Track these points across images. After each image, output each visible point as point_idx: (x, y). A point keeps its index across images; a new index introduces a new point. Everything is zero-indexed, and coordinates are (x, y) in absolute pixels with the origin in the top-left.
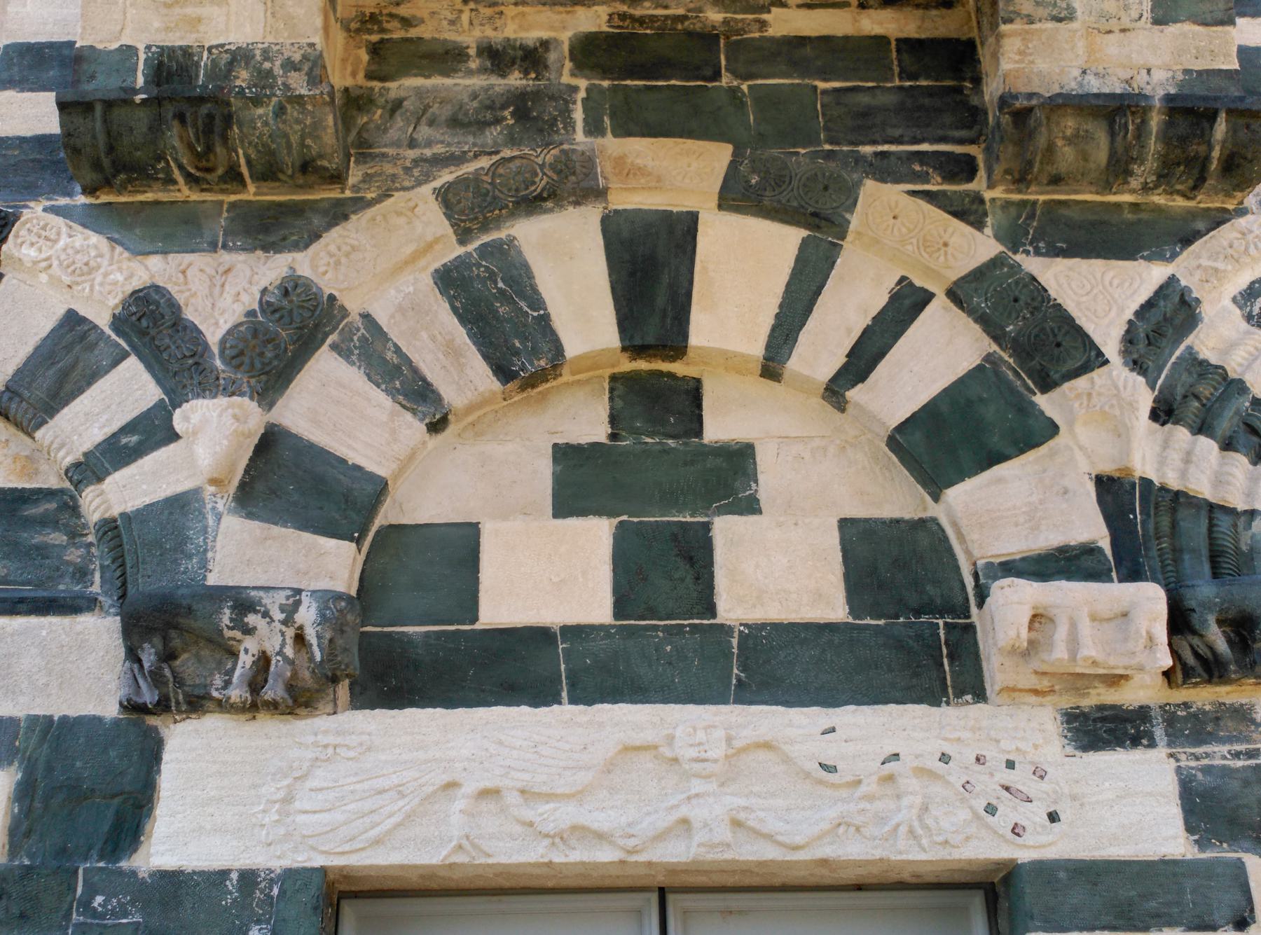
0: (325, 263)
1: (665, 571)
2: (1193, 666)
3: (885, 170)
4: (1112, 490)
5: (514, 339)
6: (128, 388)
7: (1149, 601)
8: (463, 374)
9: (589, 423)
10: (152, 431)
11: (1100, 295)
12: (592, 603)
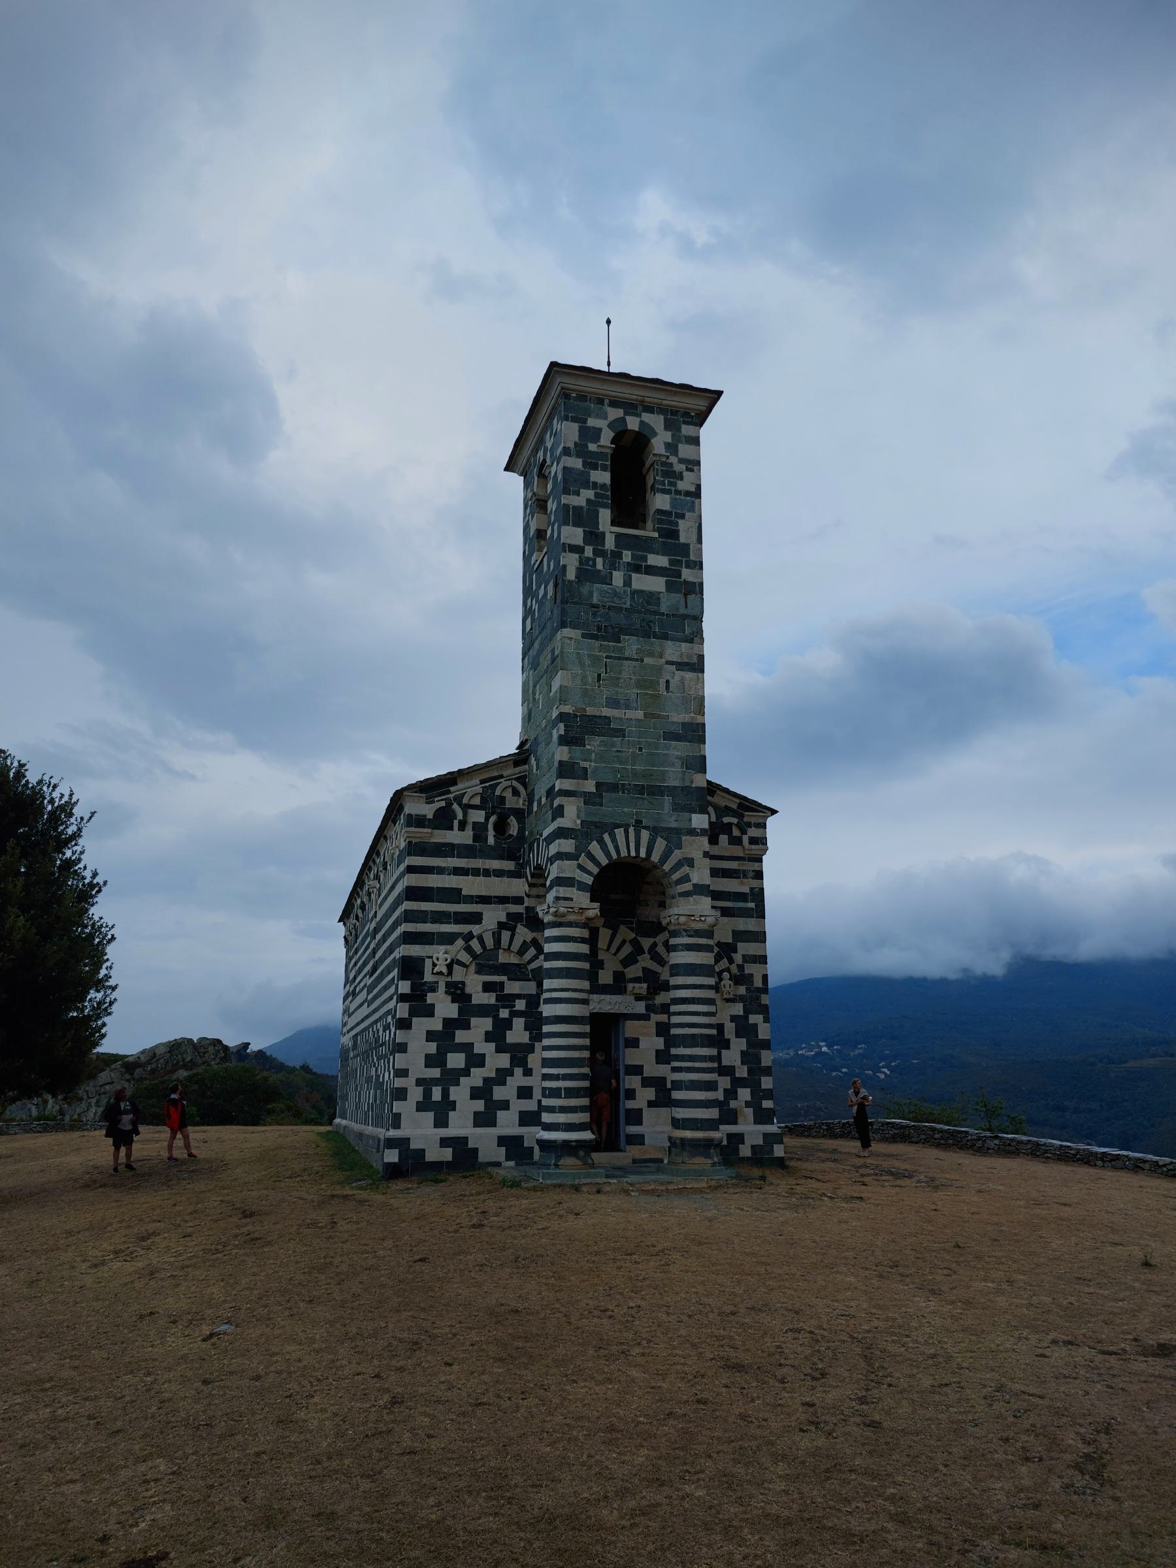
2: (649, 992)
3: (624, 923)
4: (644, 969)
7: (645, 985)
11: (646, 943)
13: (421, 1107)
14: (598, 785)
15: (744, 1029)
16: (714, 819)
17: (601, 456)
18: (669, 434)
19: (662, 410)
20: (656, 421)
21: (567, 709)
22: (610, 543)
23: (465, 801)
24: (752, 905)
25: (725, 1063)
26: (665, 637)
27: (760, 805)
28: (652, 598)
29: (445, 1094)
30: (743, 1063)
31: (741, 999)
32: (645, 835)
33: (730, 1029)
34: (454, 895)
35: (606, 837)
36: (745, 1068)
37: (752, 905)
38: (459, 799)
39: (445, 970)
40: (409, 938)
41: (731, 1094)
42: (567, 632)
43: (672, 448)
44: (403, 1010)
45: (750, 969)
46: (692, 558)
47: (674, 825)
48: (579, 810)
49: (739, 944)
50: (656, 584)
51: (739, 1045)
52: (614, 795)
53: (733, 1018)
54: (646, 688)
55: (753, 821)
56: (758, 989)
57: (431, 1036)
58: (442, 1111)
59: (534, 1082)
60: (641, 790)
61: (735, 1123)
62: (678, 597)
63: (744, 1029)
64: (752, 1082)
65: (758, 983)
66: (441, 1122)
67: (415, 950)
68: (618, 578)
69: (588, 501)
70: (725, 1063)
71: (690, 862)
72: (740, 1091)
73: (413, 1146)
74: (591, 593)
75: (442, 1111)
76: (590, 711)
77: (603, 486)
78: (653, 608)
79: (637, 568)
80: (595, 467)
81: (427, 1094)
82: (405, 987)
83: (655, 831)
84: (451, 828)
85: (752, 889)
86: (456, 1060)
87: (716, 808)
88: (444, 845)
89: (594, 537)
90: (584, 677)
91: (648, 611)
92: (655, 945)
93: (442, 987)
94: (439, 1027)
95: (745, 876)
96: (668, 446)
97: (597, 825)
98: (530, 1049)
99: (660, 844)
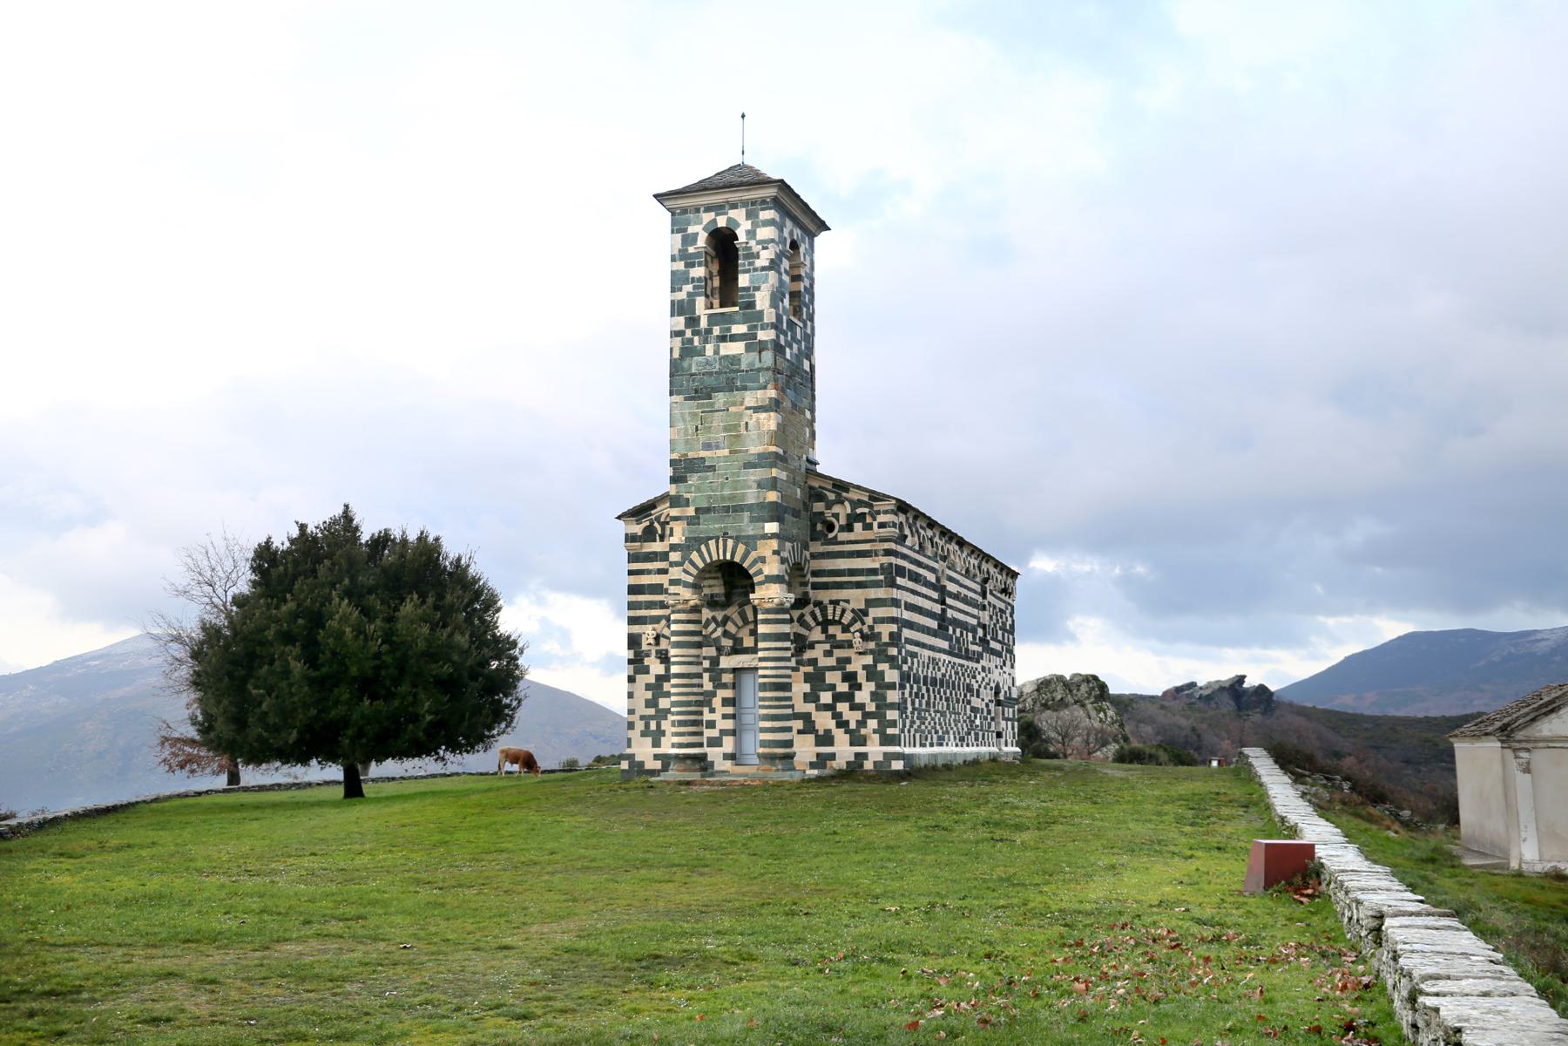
8: (740, 623)
13: (644, 734)
14: (697, 510)
15: (872, 673)
17: (697, 255)
19: (744, 204)
20: (739, 215)
21: (675, 456)
24: (881, 577)
25: (857, 700)
26: (745, 388)
28: (735, 359)
29: (659, 725)
31: (872, 652)
32: (730, 543)
34: (658, 589)
37: (881, 577)
38: (658, 519)
41: (862, 723)
42: (676, 398)
43: (751, 234)
50: (736, 348)
51: (869, 687)
53: (865, 667)
56: (887, 645)
57: (648, 687)
58: (657, 737)
59: (716, 717)
61: (864, 744)
62: (755, 355)
64: (879, 715)
65: (885, 639)
66: (656, 744)
67: (636, 629)
69: (689, 294)
70: (857, 700)
71: (763, 560)
73: (637, 759)
76: (691, 455)
77: (699, 279)
79: (723, 339)
80: (692, 265)
81: (647, 725)
83: (737, 539)
86: (664, 703)
87: (851, 502)
89: (692, 321)
90: (686, 430)
91: (732, 371)
92: (802, 615)
96: (748, 232)
97: (695, 539)
98: (714, 694)
99: (741, 548)
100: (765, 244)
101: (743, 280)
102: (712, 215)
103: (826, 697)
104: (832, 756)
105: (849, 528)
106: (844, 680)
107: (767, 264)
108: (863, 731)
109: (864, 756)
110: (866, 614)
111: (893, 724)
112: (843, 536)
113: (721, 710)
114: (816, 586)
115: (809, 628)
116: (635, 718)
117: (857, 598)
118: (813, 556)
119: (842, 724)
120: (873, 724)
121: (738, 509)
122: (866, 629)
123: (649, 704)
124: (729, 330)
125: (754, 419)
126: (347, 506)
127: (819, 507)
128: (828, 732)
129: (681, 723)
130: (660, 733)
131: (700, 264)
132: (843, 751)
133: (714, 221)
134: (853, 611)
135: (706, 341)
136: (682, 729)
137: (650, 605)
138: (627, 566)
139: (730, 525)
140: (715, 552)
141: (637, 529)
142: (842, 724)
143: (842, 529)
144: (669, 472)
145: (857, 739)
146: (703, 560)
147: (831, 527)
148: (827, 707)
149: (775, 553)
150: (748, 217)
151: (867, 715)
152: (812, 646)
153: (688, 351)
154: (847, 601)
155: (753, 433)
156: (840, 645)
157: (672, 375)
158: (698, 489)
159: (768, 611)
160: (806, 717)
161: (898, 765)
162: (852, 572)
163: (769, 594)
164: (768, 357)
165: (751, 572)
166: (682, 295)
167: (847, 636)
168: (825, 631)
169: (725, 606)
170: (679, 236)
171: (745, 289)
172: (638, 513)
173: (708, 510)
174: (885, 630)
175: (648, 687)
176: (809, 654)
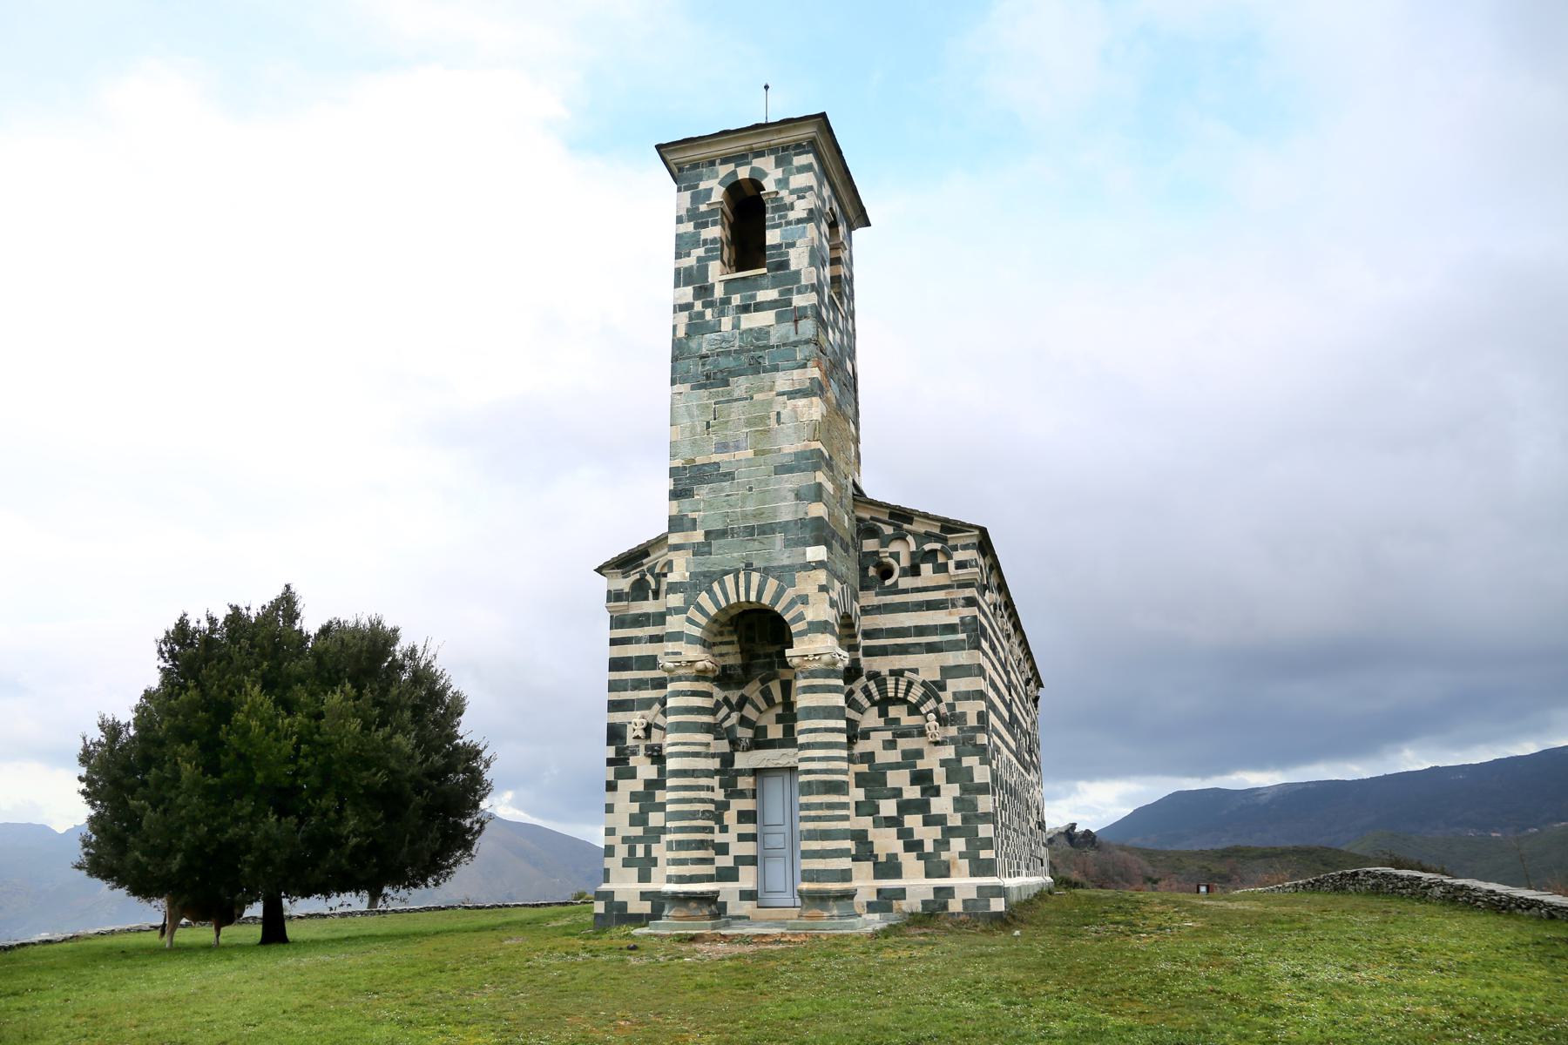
0: (747, 691)
1: (789, 731)
5: (770, 702)
6: (725, 710)
8: (763, 706)
9: (779, 710)
10: (728, 716)
12: (780, 735)
14: (707, 534)
15: (955, 771)
16: (913, 548)
18: (780, 170)
19: (773, 150)
20: (766, 163)
21: (678, 463)
22: (719, 292)
23: (657, 570)
24: (963, 636)
26: (776, 369)
27: (963, 524)
28: (763, 333)
29: (648, 850)
30: (955, 810)
31: (953, 740)
33: (939, 776)
34: (650, 662)
35: (716, 586)
36: (959, 816)
37: (963, 636)
38: (651, 570)
39: (641, 734)
40: (614, 706)
41: (942, 844)
42: (679, 388)
43: (783, 182)
44: (610, 773)
45: (961, 707)
46: (803, 282)
47: (786, 562)
48: (688, 563)
49: (949, 681)
52: (722, 541)
53: (943, 763)
54: (755, 425)
55: (960, 543)
56: (973, 729)
57: (634, 797)
58: (645, 867)
59: (730, 838)
60: (750, 531)
61: (947, 875)
62: (788, 327)
63: (955, 771)
64: (967, 831)
65: (972, 721)
66: (644, 877)
67: (619, 717)
68: (726, 323)
69: (699, 259)
71: (804, 600)
72: (953, 841)
74: (700, 345)
75: (645, 867)
76: (699, 460)
77: (714, 241)
78: (760, 343)
79: (745, 309)
80: (705, 225)
81: (632, 851)
82: (611, 752)
84: (646, 598)
85: (962, 619)
86: (655, 819)
87: (915, 534)
88: (641, 615)
89: (704, 291)
90: (693, 428)
93: (642, 750)
94: (641, 788)
95: (954, 606)
96: (778, 182)
97: (704, 575)
98: (726, 806)
99: (772, 584)
100: (801, 193)
101: (772, 237)
102: (731, 167)
103: (888, 808)
104: (901, 893)
105: (914, 571)
106: (913, 783)
107: (804, 215)
108: (944, 856)
109: (944, 893)
110: (943, 688)
111: (988, 844)
112: (906, 583)
113: (736, 828)
114: (869, 652)
115: (861, 711)
116: (616, 840)
117: (927, 666)
118: (865, 611)
119: (913, 845)
120: (958, 844)
121: (767, 530)
122: (943, 709)
123: (635, 820)
124: (754, 297)
125: (787, 407)
126: (288, 587)
127: (870, 545)
128: (892, 857)
129: (681, 845)
130: (651, 861)
131: (714, 223)
132: (916, 884)
133: (734, 173)
134: (924, 684)
135: (722, 314)
136: (684, 854)
137: (638, 685)
138: (606, 633)
139: (754, 550)
140: (732, 592)
141: (624, 584)
142: (913, 845)
143: (905, 573)
144: (667, 484)
145: (936, 867)
146: (716, 603)
147: (886, 572)
148: (890, 822)
149: (823, 589)
150: (778, 165)
151: (950, 832)
152: (866, 735)
153: (697, 327)
154: (915, 671)
155: (788, 426)
156: (906, 734)
157: (675, 359)
158: (710, 505)
159: (813, 674)
160: (860, 837)
161: (998, 905)
162: (921, 630)
163: (813, 648)
164: (808, 327)
165: (787, 618)
166: (690, 261)
167: (915, 720)
168: (883, 713)
169: (741, 684)
170: (688, 193)
171: (773, 247)
172: (627, 562)
173: (723, 533)
174: (971, 709)
175: (634, 797)
176: (861, 747)
